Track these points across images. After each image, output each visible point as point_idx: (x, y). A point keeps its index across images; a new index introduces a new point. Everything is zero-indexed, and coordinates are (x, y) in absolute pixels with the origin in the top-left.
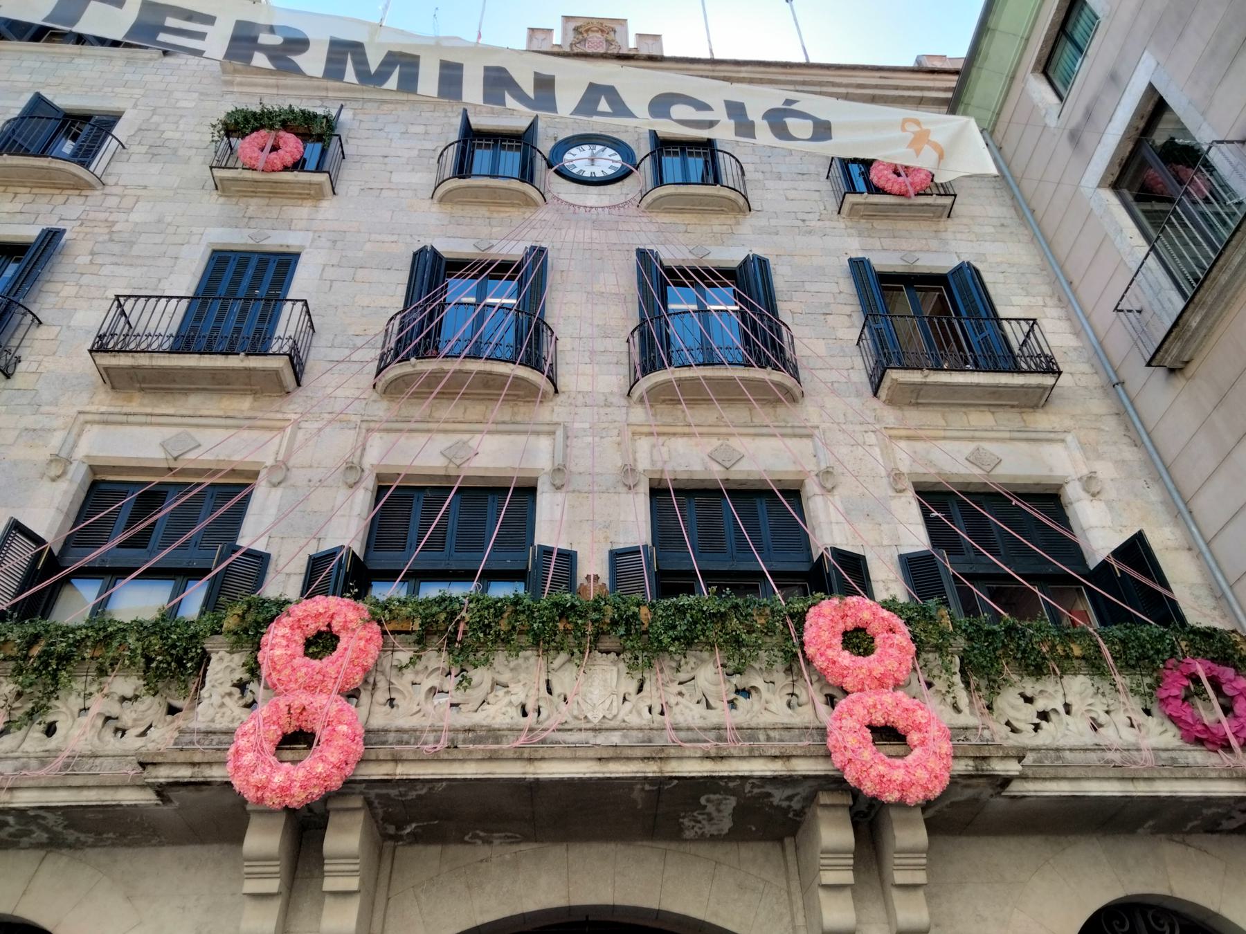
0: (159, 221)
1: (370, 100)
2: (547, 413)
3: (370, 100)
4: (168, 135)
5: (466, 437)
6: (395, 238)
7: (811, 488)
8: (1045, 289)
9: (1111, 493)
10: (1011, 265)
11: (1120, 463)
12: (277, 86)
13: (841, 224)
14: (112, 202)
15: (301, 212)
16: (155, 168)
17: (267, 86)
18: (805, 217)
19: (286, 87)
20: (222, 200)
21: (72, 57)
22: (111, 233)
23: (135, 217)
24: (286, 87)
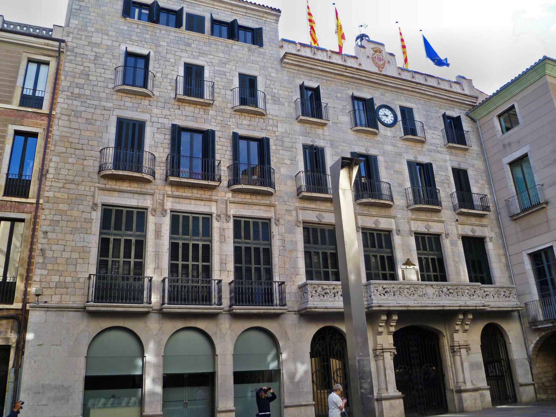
0: (286, 132)
1: (324, 79)
2: (393, 212)
3: (324, 79)
4: (274, 91)
5: (377, 218)
6: (345, 145)
7: (444, 235)
8: (485, 178)
9: (494, 241)
10: (479, 169)
11: (496, 233)
12: (298, 70)
13: (445, 150)
14: (271, 122)
15: (320, 131)
16: (276, 107)
17: (295, 70)
18: (437, 145)
19: (301, 71)
20: (299, 124)
21: (232, 45)
22: (276, 136)
23: (280, 130)
24: (301, 71)
